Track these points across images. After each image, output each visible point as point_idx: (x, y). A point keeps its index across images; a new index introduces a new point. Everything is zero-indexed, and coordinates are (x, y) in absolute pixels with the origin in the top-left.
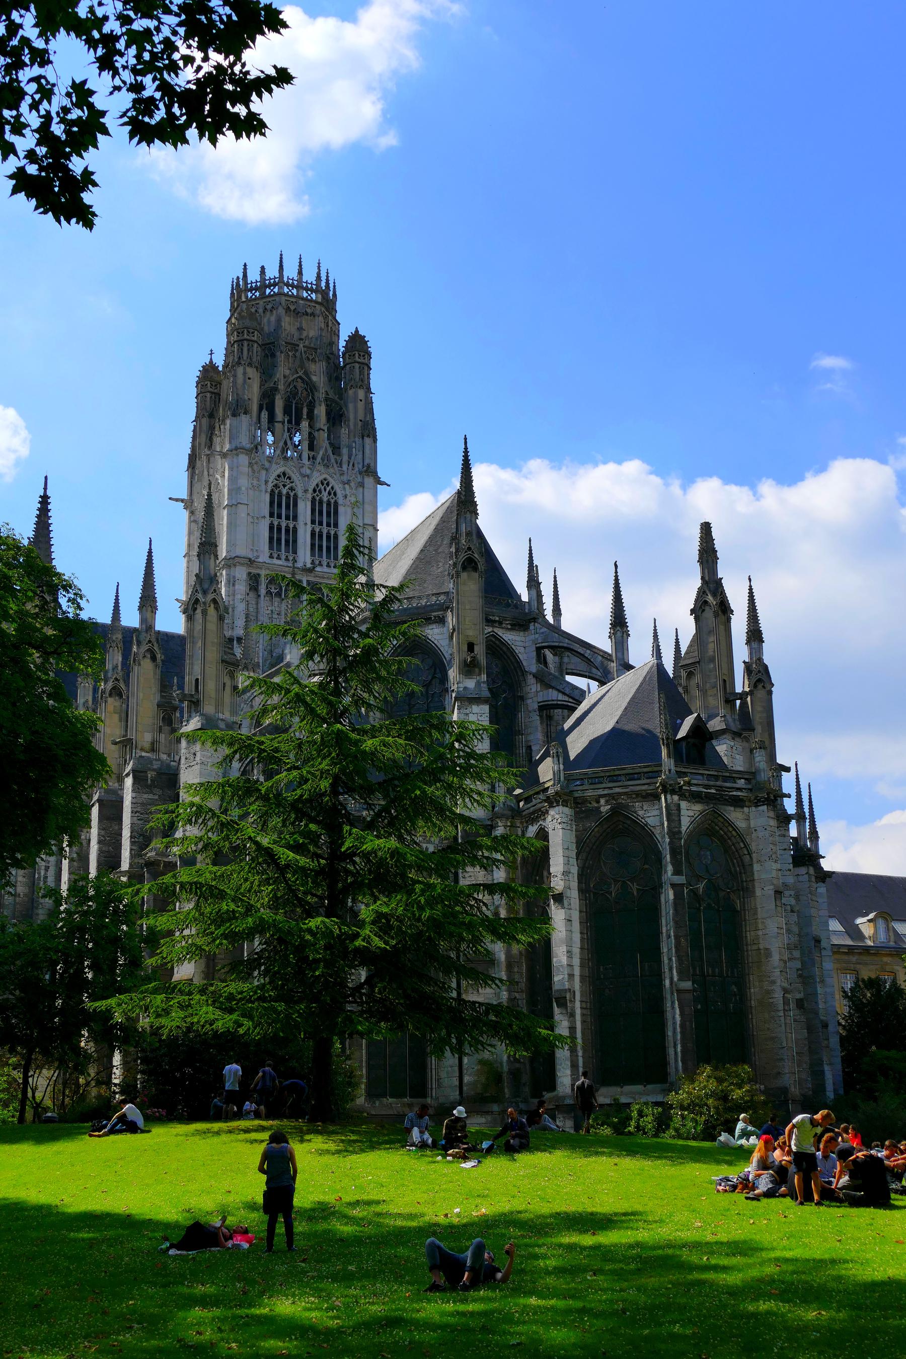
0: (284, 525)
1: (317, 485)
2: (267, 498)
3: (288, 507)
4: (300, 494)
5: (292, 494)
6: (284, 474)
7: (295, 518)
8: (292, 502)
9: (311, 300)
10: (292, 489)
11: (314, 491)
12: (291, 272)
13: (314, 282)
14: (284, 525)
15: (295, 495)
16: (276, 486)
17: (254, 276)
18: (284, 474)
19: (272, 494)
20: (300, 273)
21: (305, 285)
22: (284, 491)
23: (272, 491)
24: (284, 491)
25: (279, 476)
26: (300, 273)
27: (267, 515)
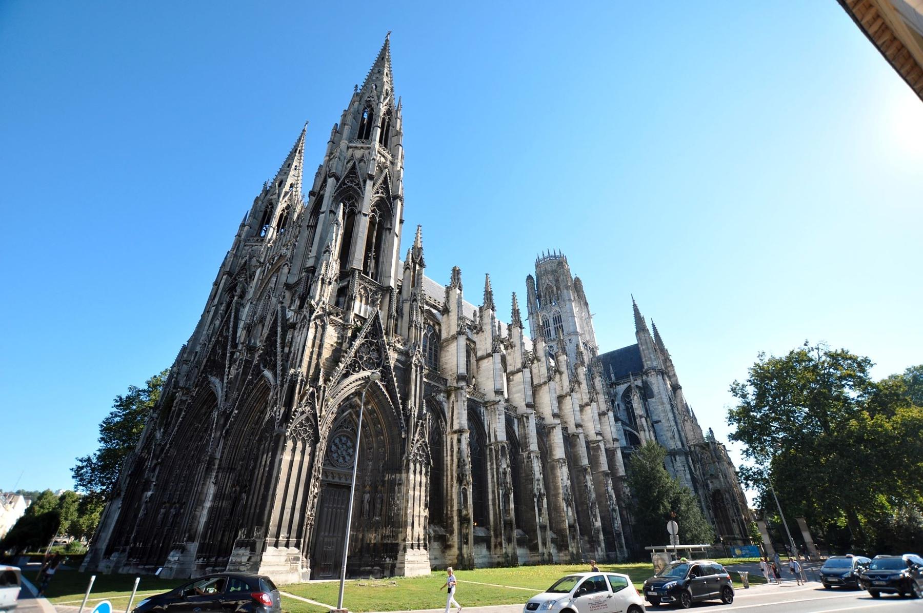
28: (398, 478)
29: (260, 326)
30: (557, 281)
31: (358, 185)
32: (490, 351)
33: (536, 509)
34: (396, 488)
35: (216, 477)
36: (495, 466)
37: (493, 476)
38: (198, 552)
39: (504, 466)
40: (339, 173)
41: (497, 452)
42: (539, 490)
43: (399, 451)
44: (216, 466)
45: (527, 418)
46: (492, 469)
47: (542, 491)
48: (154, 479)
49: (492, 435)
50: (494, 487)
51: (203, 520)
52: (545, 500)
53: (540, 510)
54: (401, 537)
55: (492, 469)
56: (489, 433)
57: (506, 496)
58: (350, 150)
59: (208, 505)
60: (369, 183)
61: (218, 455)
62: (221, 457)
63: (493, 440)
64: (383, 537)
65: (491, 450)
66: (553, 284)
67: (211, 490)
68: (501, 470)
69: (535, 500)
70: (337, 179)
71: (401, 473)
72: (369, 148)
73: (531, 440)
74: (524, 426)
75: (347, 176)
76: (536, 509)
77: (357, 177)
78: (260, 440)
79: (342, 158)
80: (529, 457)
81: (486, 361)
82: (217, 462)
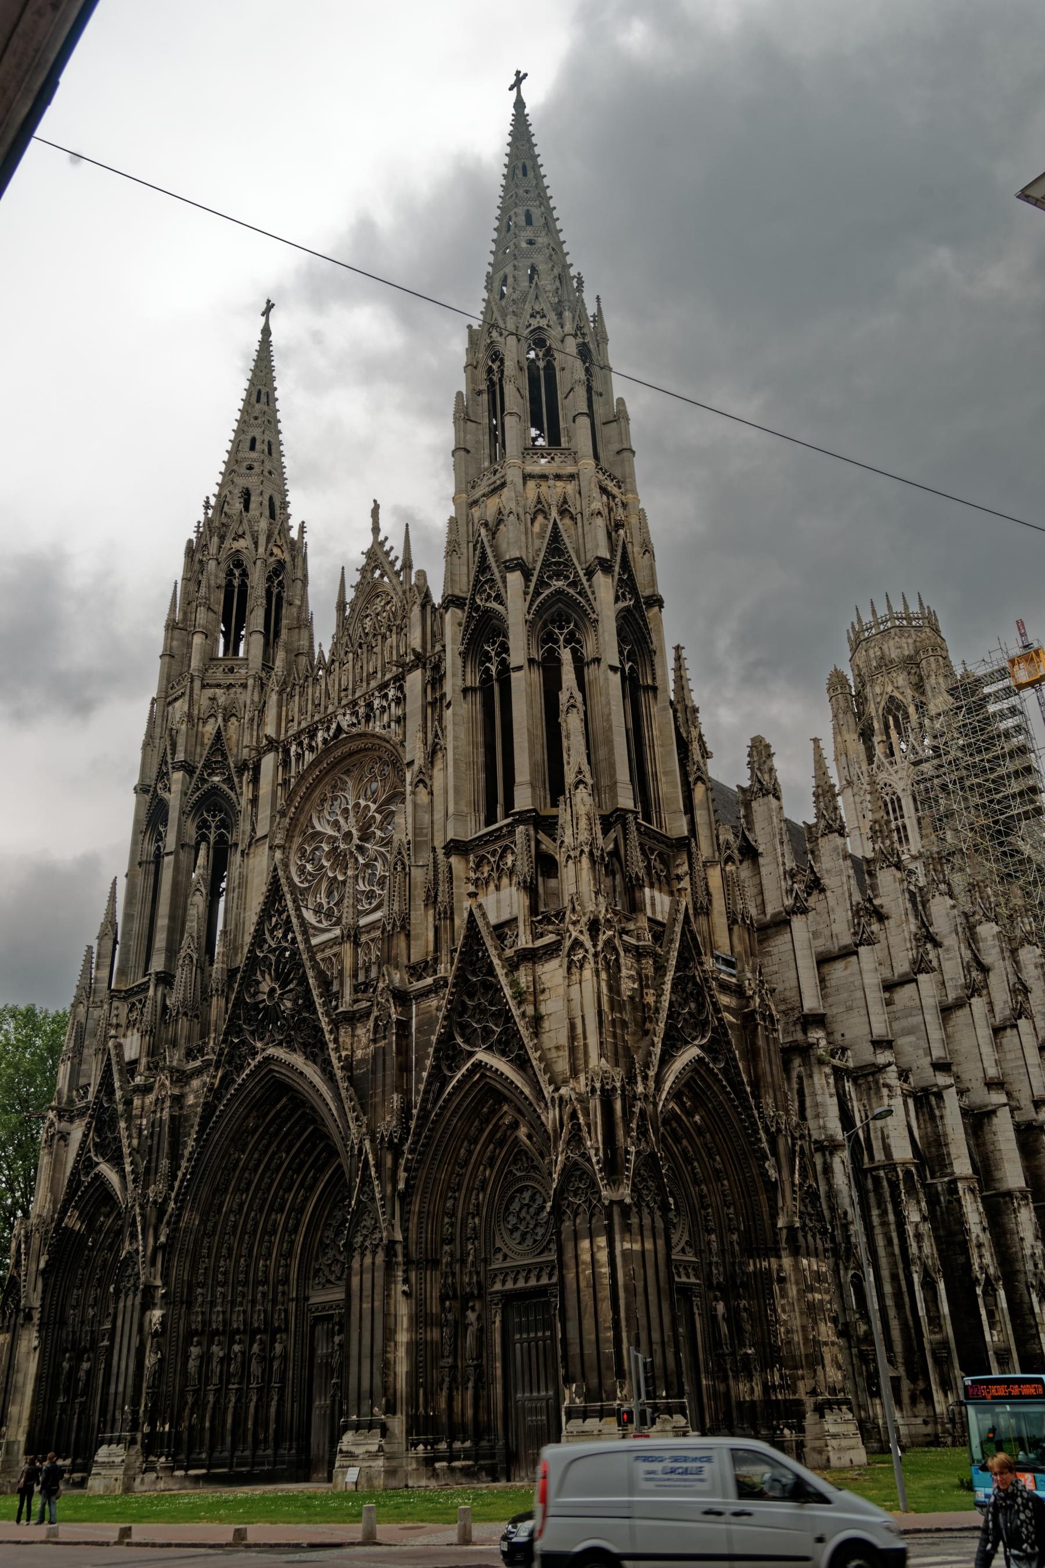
3: (894, 811)
7: (902, 817)
12: (867, 618)
20: (874, 612)
22: (888, 799)
26: (874, 612)
28: (775, 1267)
29: (402, 937)
30: (919, 687)
31: (574, 584)
32: (847, 939)
33: (983, 1312)
34: (776, 1287)
35: (406, 1281)
36: (891, 1218)
37: (889, 1242)
38: (409, 1433)
39: (915, 1217)
40: (528, 557)
41: (894, 1186)
42: (983, 1268)
43: (765, 1209)
44: (400, 1259)
45: (939, 1096)
46: (884, 1224)
47: (991, 1270)
48: (158, 1282)
49: (877, 1145)
50: (893, 1265)
51: (402, 1368)
52: (1002, 1293)
53: (991, 1314)
54: (803, 1387)
55: (884, 1224)
56: (868, 1139)
57: (929, 1285)
58: (531, 484)
59: (403, 1337)
60: (600, 577)
61: (399, 1236)
62: (406, 1239)
63: (879, 1156)
64: (767, 1388)
65: (877, 1180)
66: (908, 697)
67: (403, 1309)
68: (910, 1229)
69: (979, 1291)
70: (527, 575)
71: (779, 1257)
72: (572, 477)
73: (953, 1150)
74: (932, 1117)
75: (546, 564)
76: (983, 1312)
77: (568, 564)
78: (557, 1212)
79: (521, 513)
80: (952, 1190)
81: (840, 965)
82: (399, 1249)
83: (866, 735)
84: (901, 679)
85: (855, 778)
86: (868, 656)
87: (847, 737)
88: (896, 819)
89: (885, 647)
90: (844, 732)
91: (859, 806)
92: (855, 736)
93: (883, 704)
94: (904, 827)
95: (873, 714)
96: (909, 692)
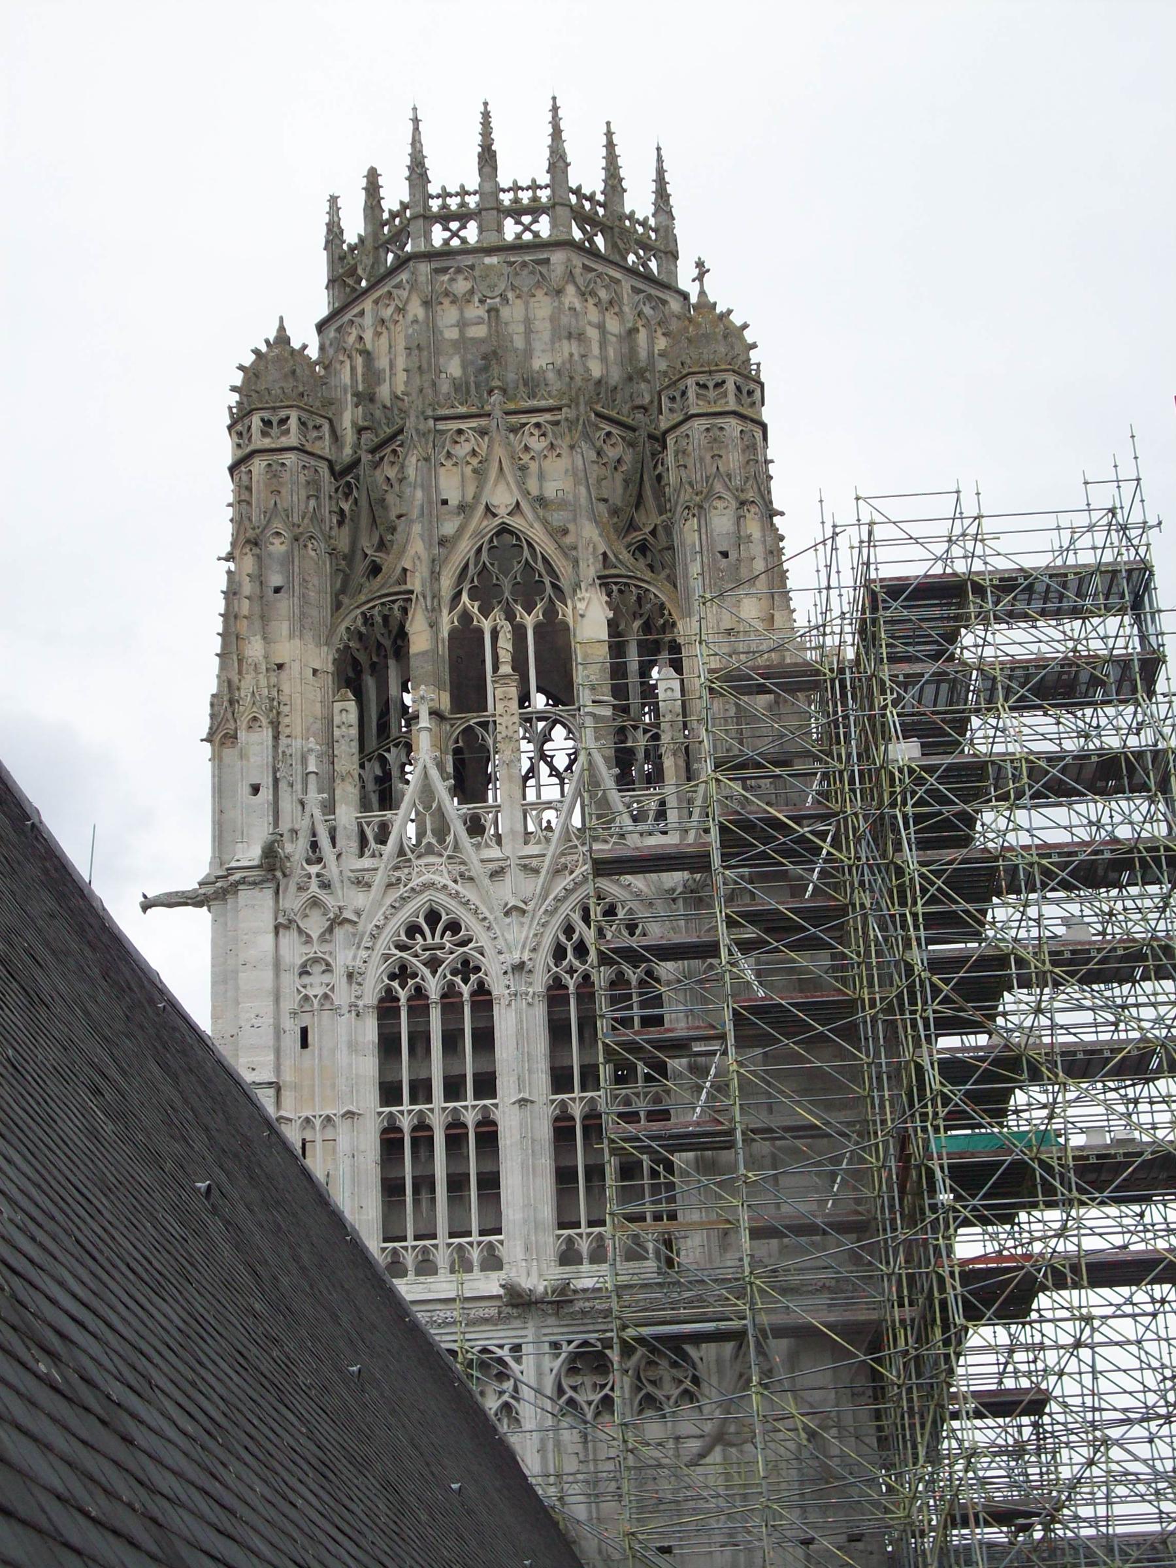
0: (438, 1123)
1: (569, 930)
2: (370, 1030)
3: (452, 1041)
4: (498, 987)
5: (466, 990)
6: (433, 917)
7: (486, 1085)
8: (472, 1017)
9: (538, 245)
10: (467, 968)
11: (559, 953)
12: (452, 171)
13: (544, 179)
14: (438, 1123)
15: (482, 990)
16: (402, 973)
17: (354, 228)
18: (433, 917)
19: (387, 1008)
20: (488, 158)
21: (506, 198)
22: (433, 986)
23: (389, 997)
24: (433, 986)
25: (413, 930)
26: (488, 158)
27: (368, 1099)
83: (368, 663)
84: (561, 473)
85: (296, 850)
86: (432, 326)
87: (287, 649)
88: (454, 1089)
89: (513, 313)
90: (282, 628)
91: (290, 981)
92: (323, 658)
93: (464, 549)
94: (488, 1137)
95: (416, 583)
96: (590, 536)
